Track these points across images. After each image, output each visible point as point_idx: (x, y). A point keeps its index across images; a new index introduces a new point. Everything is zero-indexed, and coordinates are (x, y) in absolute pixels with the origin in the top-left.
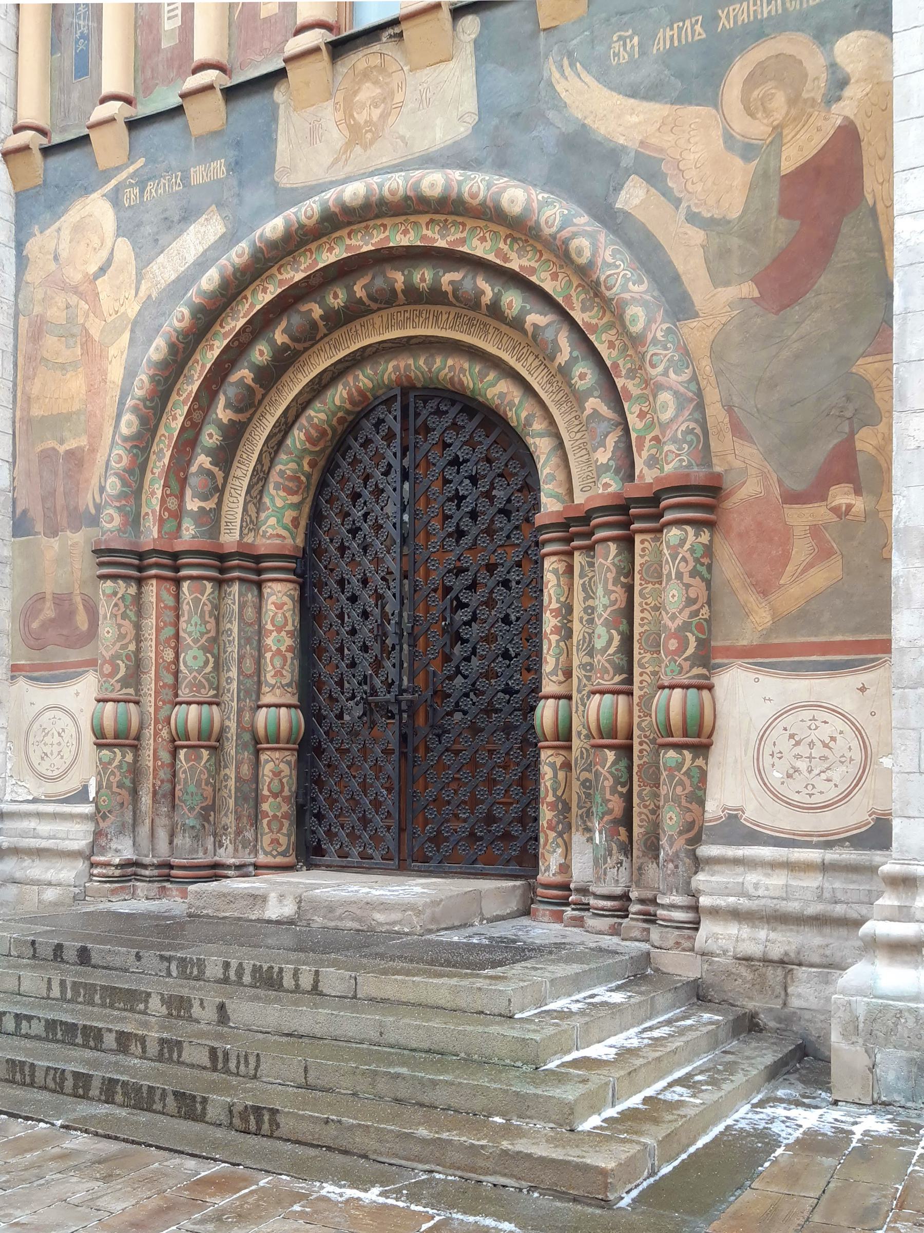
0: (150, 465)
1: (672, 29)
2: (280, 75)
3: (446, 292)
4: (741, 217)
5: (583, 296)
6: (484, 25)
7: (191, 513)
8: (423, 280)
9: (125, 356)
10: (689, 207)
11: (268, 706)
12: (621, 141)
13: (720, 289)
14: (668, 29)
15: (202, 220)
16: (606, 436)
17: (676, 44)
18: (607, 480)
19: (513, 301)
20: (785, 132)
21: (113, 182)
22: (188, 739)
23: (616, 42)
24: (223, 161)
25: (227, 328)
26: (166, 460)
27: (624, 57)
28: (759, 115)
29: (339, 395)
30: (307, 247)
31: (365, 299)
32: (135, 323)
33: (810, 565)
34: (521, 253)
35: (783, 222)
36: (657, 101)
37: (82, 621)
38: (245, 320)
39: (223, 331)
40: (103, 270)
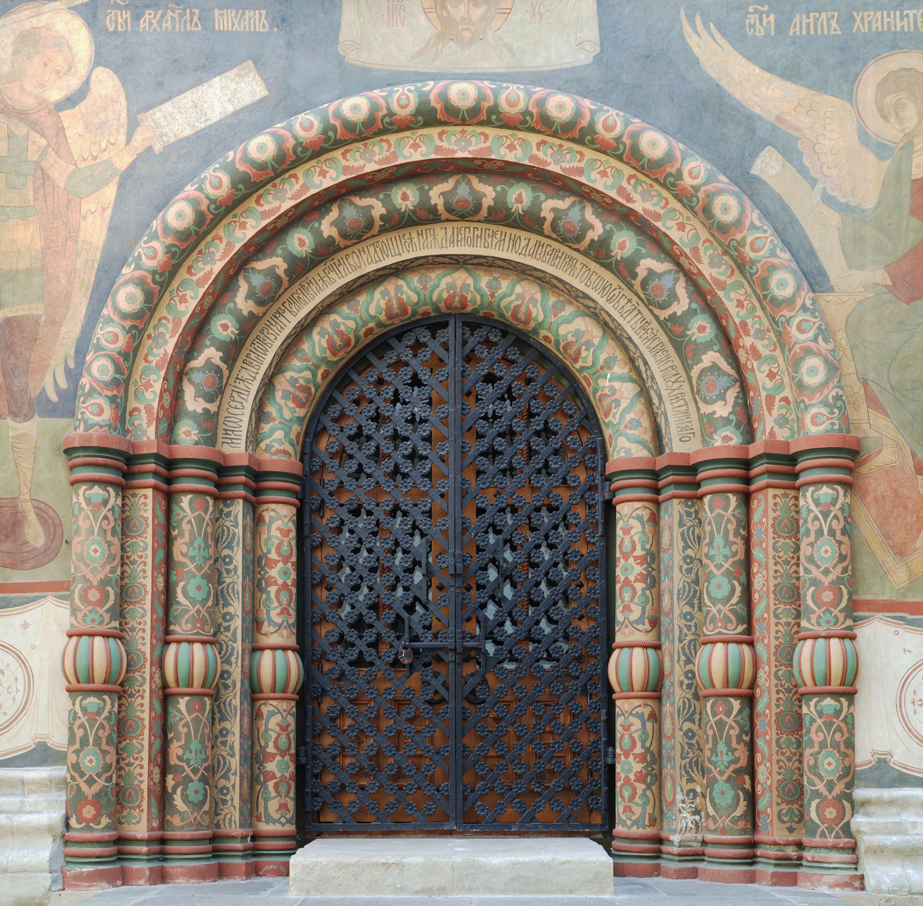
0: (143, 351)
1: (808, 17)
3: (545, 219)
4: (875, 209)
5: (710, 252)
8: (519, 200)
9: (108, 213)
10: (824, 188)
12: (757, 110)
13: (854, 272)
14: (804, 16)
15: (232, 74)
16: (726, 391)
17: (812, 32)
18: (728, 433)
20: (916, 141)
23: (753, 13)
24: (264, 12)
25: (267, 207)
26: (170, 348)
27: (760, 32)
28: (892, 120)
30: (384, 137)
31: (441, 208)
35: (914, 222)
36: (794, 82)
38: (294, 202)
39: (260, 209)
40: (72, 100)
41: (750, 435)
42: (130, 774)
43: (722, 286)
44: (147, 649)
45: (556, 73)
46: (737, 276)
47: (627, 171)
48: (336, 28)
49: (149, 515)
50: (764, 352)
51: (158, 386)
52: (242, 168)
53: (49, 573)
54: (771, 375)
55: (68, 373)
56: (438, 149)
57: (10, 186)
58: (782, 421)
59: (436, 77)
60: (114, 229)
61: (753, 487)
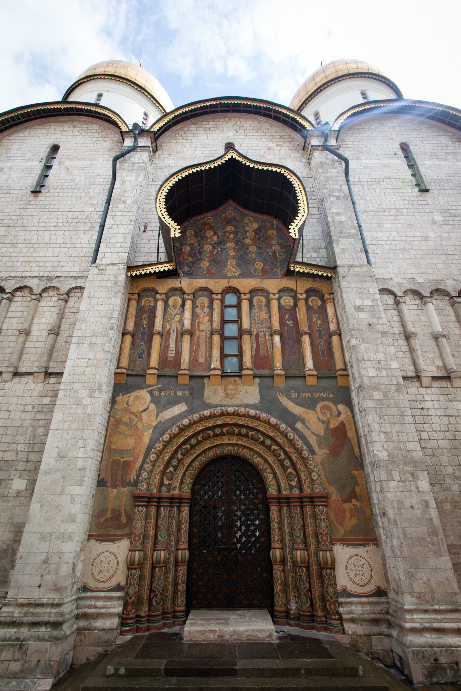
0: (155, 469)
2: (209, 377)
6: (261, 381)
7: (166, 485)
11: (182, 549)
19: (268, 442)
21: (151, 388)
22: (159, 564)
26: (161, 468)
27: (294, 397)
29: (210, 454)
32: (155, 428)
33: (351, 518)
34: (272, 432)
35: (333, 439)
37: (124, 519)
40: (144, 411)
41: (301, 490)
42: (141, 594)
43: (291, 453)
44: (149, 553)
45: (251, 405)
46: (294, 451)
47: (268, 426)
48: (203, 395)
49: (153, 513)
50: (303, 469)
51: (158, 478)
52: (181, 426)
53: (126, 531)
54: (305, 475)
55: (137, 475)
56: (225, 421)
57: (129, 429)
58: (308, 487)
59: (225, 406)
60: (151, 439)
61: (304, 504)
